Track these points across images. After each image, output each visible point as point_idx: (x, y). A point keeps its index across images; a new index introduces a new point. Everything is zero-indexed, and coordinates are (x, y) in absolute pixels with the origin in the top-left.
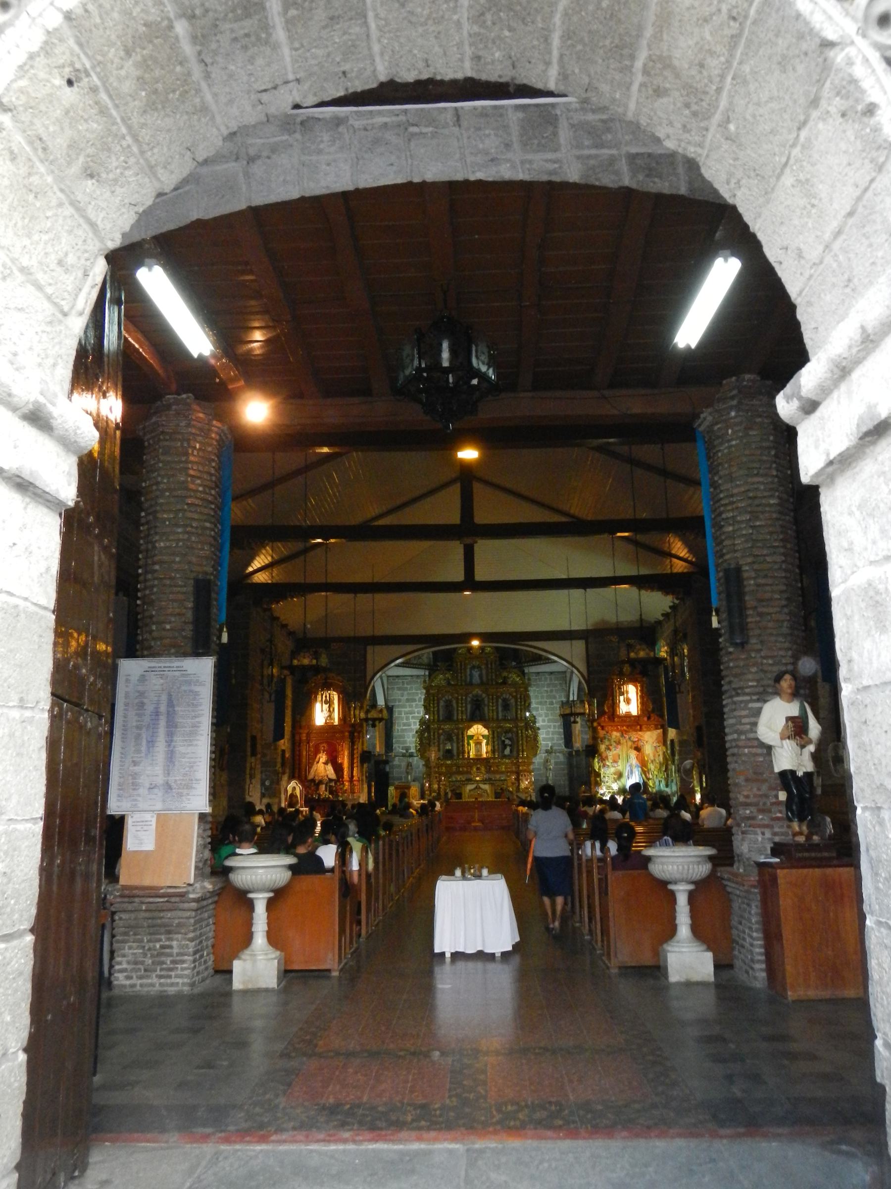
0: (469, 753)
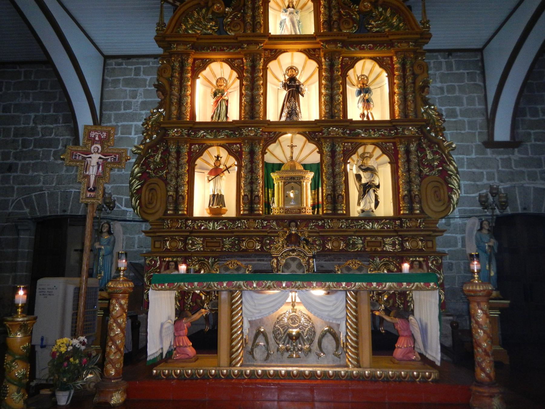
0: (268, 205)
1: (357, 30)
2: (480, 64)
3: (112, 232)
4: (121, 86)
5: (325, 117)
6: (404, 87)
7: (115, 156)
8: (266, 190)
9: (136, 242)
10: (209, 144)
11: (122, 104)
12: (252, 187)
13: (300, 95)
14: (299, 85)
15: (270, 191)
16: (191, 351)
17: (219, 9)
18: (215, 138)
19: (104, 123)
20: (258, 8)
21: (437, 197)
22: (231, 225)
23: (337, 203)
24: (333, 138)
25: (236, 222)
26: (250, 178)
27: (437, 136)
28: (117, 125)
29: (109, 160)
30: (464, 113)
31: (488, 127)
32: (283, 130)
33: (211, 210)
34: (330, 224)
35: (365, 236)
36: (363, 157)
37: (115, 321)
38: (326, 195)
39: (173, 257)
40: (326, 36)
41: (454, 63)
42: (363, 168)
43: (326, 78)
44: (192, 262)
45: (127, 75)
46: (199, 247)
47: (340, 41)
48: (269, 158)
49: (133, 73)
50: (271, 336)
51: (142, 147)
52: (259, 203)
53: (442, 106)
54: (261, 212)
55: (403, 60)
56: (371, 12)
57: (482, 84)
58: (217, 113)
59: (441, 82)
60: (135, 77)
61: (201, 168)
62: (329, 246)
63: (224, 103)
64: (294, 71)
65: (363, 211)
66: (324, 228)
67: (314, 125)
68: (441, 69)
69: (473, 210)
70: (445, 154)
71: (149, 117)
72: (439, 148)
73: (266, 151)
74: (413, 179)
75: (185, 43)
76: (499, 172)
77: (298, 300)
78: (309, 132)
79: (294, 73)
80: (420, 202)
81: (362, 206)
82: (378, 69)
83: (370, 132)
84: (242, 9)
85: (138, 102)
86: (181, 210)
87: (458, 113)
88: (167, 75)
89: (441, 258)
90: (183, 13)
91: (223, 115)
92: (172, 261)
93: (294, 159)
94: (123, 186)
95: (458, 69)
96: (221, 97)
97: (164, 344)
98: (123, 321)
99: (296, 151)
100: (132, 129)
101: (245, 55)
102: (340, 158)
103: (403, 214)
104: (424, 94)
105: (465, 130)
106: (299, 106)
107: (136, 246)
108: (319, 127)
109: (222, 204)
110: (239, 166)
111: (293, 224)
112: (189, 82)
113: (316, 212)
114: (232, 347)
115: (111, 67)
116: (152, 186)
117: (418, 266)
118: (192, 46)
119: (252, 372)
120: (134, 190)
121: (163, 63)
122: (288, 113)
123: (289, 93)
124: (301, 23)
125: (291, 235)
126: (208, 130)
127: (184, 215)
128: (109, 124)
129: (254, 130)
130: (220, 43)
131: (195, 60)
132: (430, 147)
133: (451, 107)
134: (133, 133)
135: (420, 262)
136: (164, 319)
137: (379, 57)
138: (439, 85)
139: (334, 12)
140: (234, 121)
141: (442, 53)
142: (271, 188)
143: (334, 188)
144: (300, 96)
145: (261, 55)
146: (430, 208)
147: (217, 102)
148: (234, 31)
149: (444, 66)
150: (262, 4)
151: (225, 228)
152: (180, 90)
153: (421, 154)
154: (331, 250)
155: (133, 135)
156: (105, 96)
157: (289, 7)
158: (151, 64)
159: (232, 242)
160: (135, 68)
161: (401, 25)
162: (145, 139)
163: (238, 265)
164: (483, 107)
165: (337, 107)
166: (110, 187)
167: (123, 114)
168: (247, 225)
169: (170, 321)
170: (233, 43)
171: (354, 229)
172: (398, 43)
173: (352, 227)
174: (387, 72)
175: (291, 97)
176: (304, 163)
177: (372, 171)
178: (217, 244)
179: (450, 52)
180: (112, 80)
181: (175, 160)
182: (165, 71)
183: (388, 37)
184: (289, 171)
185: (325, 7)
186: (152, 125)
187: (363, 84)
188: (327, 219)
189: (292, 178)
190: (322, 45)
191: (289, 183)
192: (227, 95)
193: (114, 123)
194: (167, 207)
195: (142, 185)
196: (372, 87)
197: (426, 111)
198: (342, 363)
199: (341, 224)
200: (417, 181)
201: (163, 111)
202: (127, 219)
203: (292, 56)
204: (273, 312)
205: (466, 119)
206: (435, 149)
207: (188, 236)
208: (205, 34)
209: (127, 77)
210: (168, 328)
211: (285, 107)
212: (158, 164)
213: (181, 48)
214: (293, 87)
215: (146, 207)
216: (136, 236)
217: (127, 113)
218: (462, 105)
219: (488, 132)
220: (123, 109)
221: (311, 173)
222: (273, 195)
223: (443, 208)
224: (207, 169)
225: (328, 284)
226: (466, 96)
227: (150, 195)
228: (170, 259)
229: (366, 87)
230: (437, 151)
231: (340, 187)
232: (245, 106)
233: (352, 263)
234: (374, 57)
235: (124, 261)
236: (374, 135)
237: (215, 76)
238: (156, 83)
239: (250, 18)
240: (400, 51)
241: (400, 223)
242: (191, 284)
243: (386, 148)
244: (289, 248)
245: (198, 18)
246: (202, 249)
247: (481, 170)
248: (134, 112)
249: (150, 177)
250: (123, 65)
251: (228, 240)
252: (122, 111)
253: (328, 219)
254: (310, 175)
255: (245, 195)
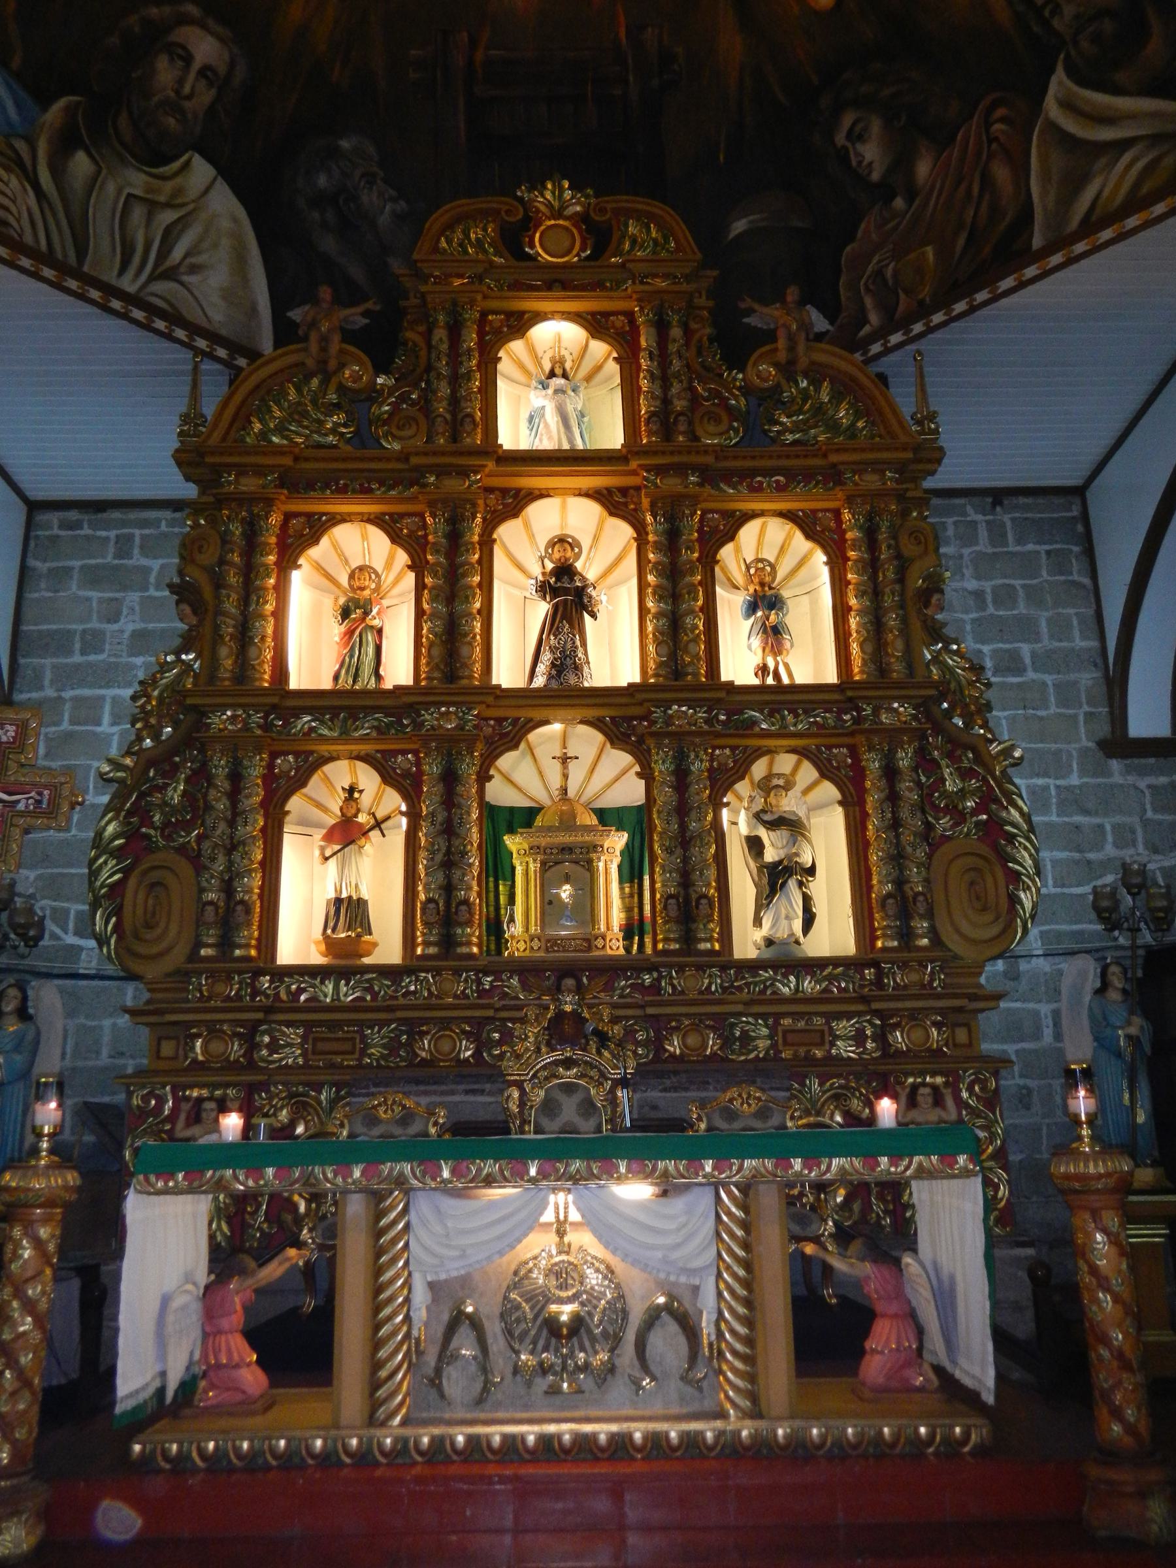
0: (495, 929)
1: (742, 438)
2: (1080, 528)
3: (31, 1011)
4: (74, 587)
5: (656, 675)
6: (873, 592)
7: (40, 794)
8: (491, 885)
9: (106, 1039)
10: (326, 754)
11: (77, 638)
12: (448, 877)
13: (586, 616)
14: (584, 588)
15: (501, 888)
16: (252, 1379)
17: (356, 378)
18: (345, 736)
19: (21, 692)
20: (469, 376)
21: (978, 898)
22: (388, 987)
23: (694, 921)
24: (678, 736)
25: (402, 980)
26: (444, 849)
27: (968, 725)
28: (60, 698)
29: (21, 806)
30: (1042, 662)
31: (1111, 698)
32: (537, 714)
33: (331, 945)
34: (675, 982)
35: (778, 1016)
36: (766, 786)
37: (19, 1293)
38: (662, 896)
39: (214, 1086)
40: (655, 453)
41: (1009, 524)
42: (767, 817)
43: (659, 569)
44: (270, 1099)
45: (94, 557)
46: (292, 1056)
47: (695, 468)
48: (499, 793)
49: (111, 549)
50: (494, 1329)
51: (128, 761)
52: (469, 923)
53: (983, 643)
54: (475, 950)
55: (870, 518)
56: (777, 389)
57: (1087, 581)
58: (350, 666)
59: (978, 578)
60: (116, 562)
61: (304, 822)
62: (674, 1046)
63: (370, 637)
64: (569, 548)
65: (769, 942)
66: (659, 994)
67: (624, 700)
68: (977, 544)
69: (1081, 933)
70: (994, 778)
71: (154, 675)
72: (978, 759)
73: (492, 772)
74: (909, 849)
75: (260, 471)
76: (1145, 823)
77: (575, 1216)
78: (612, 718)
79: (569, 554)
80: (930, 915)
81: (766, 929)
82: (800, 543)
83: (783, 718)
84: (421, 380)
85: (122, 631)
86: (240, 947)
87: (1028, 661)
88: (208, 557)
89: (996, 1074)
90: (258, 387)
91: (367, 670)
92: (210, 1099)
93: (571, 793)
94: (73, 875)
95: (1020, 541)
96: (363, 620)
97: (170, 1359)
98: (43, 1292)
99: (577, 773)
100: (102, 707)
101: (432, 504)
102: (700, 791)
103: (884, 949)
104: (929, 612)
105: (1047, 708)
106: (584, 644)
107: (105, 1052)
108: (641, 704)
109: (361, 926)
110: (413, 816)
111: (569, 982)
112: (268, 576)
113: (635, 947)
114: (377, 1365)
115: (47, 533)
116: (155, 876)
117: (930, 1100)
118: (280, 478)
119: (438, 1443)
120: (102, 886)
121: (196, 525)
122: (553, 665)
123: (556, 608)
124: (586, 419)
125: (560, 1015)
126: (324, 715)
127: (248, 959)
128: (34, 695)
129: (456, 713)
130: (362, 470)
131: (288, 517)
132: (950, 755)
133: (1007, 646)
134: (106, 719)
135: (935, 1088)
136: (171, 1282)
137: (802, 511)
138: (972, 584)
139: (676, 388)
140: (397, 688)
141: (976, 500)
142: (505, 880)
143: (686, 878)
144: (587, 617)
145: (474, 505)
146: (958, 931)
147: (350, 633)
148: (400, 439)
149: (983, 533)
150: (479, 365)
151: (369, 998)
152: (245, 601)
153: (928, 778)
154: (680, 1059)
155: (105, 727)
156: (28, 613)
157: (552, 374)
158: (163, 527)
159: (391, 1038)
160: (117, 536)
161: (860, 424)
162: (140, 739)
163: (404, 1107)
164: (1094, 644)
165: (691, 646)
166: (32, 877)
167: (77, 667)
168: (433, 988)
169: (190, 1287)
170: (392, 470)
171: (745, 995)
172: (854, 472)
173: (740, 989)
174: (827, 553)
175: (561, 622)
176: (600, 804)
177: (792, 826)
178: (347, 1046)
179: (998, 496)
180: (50, 570)
181: (225, 800)
182: (201, 547)
183: (825, 456)
184: (558, 829)
185: (652, 377)
186: (160, 699)
187: (762, 584)
188: (665, 965)
189: (566, 849)
190: (645, 478)
191: (556, 863)
192: (378, 613)
193: (50, 692)
194: (198, 936)
195: (127, 872)
196: (785, 593)
197: (936, 659)
198: (708, 1405)
199: (706, 981)
200: (920, 854)
201: (195, 660)
202: (81, 971)
203: (564, 507)
204: (501, 1253)
205: (1049, 679)
206: (966, 764)
207: (260, 1022)
208: (319, 446)
209: (93, 562)
210: (184, 1308)
211: (545, 649)
212: (175, 810)
213: (250, 484)
214: (566, 591)
215: (137, 936)
216: (107, 1023)
217: (90, 665)
218: (1038, 640)
219: (1111, 713)
220: (77, 652)
221: (620, 834)
222: (512, 900)
223: (995, 930)
224: (318, 825)
225: (661, 1165)
226: (1046, 614)
227: (150, 902)
228: (205, 1093)
229: (769, 593)
230: (971, 769)
231: (701, 874)
232: (431, 645)
233: (740, 1095)
234: (789, 511)
235: (53, 1105)
236: (795, 725)
237: (347, 562)
238: (176, 580)
239: (445, 403)
240: (859, 496)
241: (875, 974)
242: (256, 1171)
243: (829, 761)
244: (557, 1055)
245: (299, 404)
246: (300, 1061)
247: (1098, 820)
248: (112, 659)
249: (151, 848)
250: (82, 528)
251: (379, 1032)
252: (77, 659)
253: (670, 966)
254: (617, 841)
255: (429, 900)
